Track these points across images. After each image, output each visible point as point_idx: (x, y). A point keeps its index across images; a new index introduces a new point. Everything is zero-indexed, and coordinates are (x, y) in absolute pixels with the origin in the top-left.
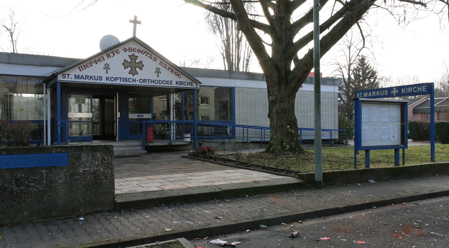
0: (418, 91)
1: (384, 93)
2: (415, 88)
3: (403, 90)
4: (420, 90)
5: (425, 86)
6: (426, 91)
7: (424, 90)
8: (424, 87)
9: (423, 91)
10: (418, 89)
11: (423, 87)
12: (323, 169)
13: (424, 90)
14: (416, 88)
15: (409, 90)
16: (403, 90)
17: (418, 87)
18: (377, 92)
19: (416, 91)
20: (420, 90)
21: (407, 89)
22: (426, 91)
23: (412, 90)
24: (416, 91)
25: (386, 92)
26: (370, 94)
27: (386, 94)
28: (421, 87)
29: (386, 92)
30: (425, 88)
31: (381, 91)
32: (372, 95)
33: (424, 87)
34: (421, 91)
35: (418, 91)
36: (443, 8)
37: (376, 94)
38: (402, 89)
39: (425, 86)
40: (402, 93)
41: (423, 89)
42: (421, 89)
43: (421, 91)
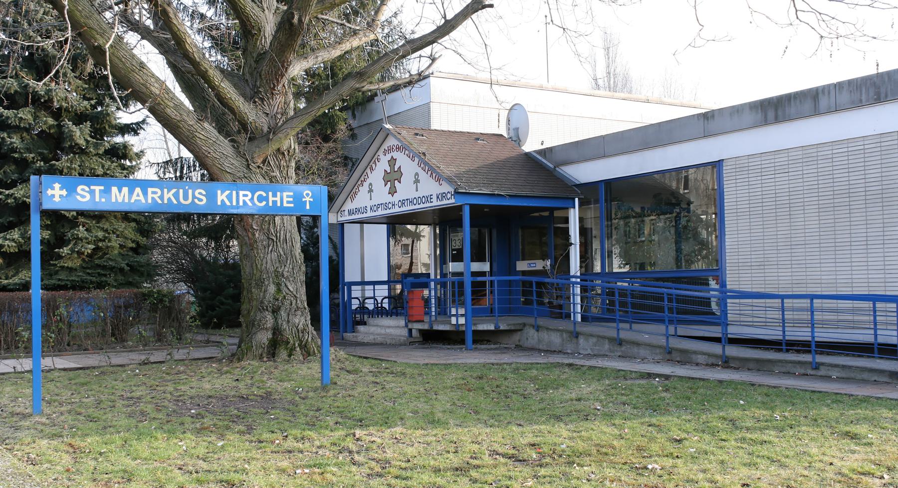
0: (271, 204)
1: (194, 197)
2: (260, 196)
3: (222, 194)
4: (275, 202)
5: (292, 194)
6: (292, 205)
7: (288, 202)
8: (288, 196)
9: (285, 205)
10: (271, 199)
11: (285, 194)
12: (42, 367)
13: (288, 202)
14: (264, 195)
15: (241, 199)
16: (222, 194)
17: (270, 194)
18: (166, 190)
19: (264, 203)
20: (275, 202)
21: (234, 193)
22: (292, 205)
23: (252, 199)
24: (264, 203)
25: (200, 193)
26: (138, 195)
27: (201, 200)
28: (278, 194)
29: (200, 193)
30: (291, 199)
31: (181, 191)
32: (146, 199)
33: (288, 196)
34: (279, 204)
35: (271, 204)
36: (804, 11)
37: (162, 197)
38: (219, 192)
39: (292, 194)
40: (219, 203)
41: (285, 200)
42: (278, 199)
43: (279, 204)
